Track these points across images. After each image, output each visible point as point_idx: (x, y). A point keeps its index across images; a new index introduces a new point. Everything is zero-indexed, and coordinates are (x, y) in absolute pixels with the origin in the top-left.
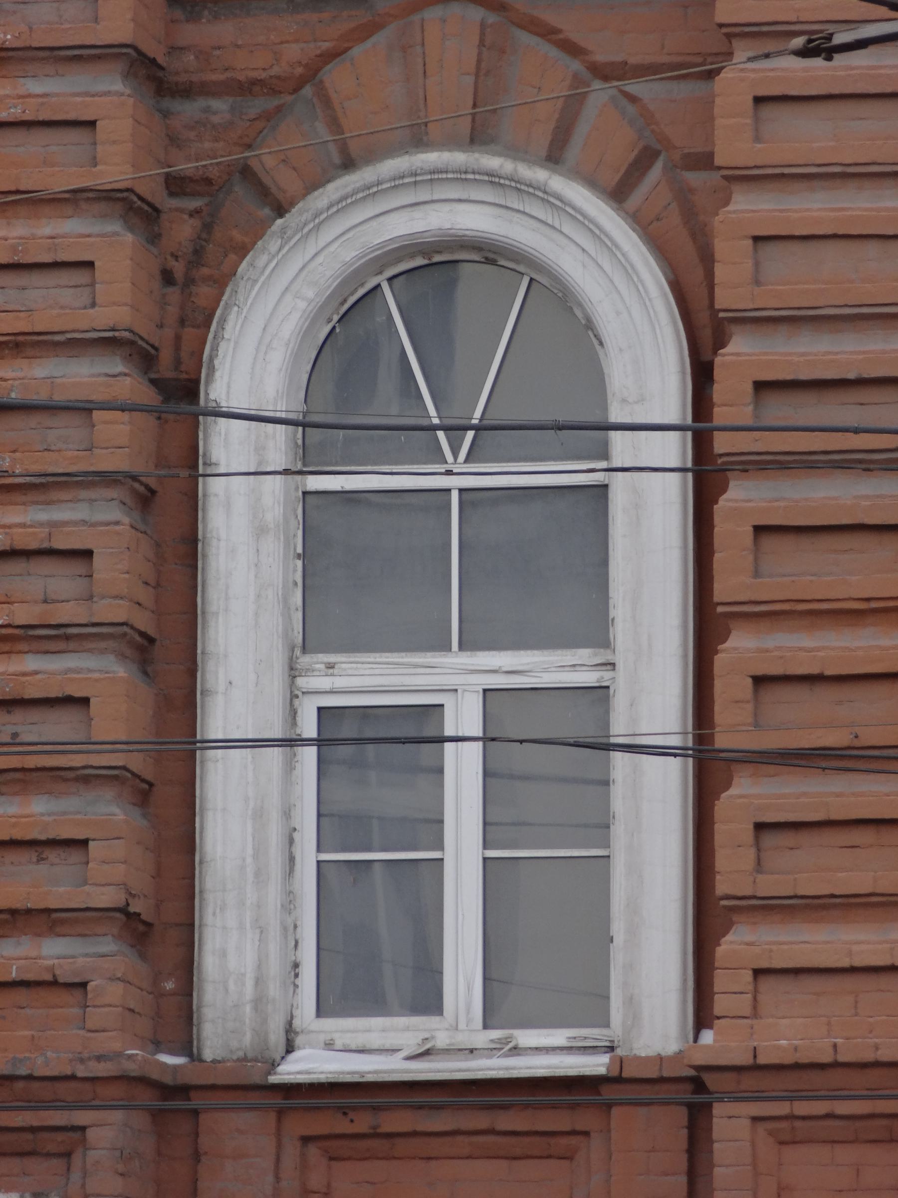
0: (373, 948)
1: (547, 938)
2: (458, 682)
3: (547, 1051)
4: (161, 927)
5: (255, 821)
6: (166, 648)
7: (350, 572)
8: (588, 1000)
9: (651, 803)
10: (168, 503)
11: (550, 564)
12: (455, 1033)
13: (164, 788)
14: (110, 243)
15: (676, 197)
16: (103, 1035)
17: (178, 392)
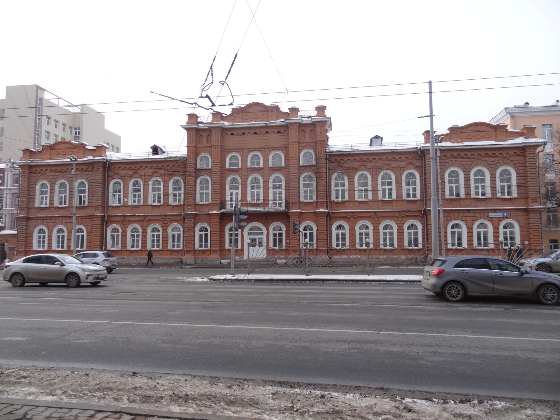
0: (202, 200)
1: (207, 200)
2: (204, 192)
3: (207, 203)
4: (195, 199)
5: (198, 196)
6: (195, 190)
7: (202, 188)
8: (208, 201)
9: (210, 196)
10: (195, 186)
11: (207, 188)
12: (204, 202)
13: (195, 195)
14: (193, 178)
15: (211, 176)
16: (193, 202)
17: (196, 182)
